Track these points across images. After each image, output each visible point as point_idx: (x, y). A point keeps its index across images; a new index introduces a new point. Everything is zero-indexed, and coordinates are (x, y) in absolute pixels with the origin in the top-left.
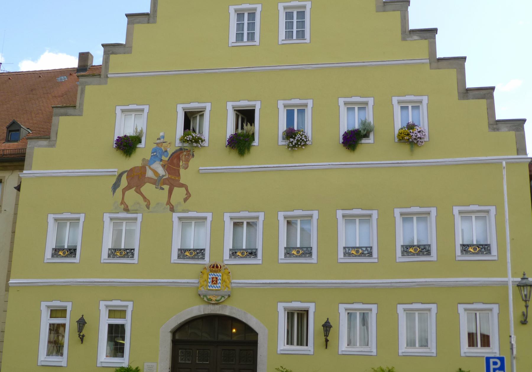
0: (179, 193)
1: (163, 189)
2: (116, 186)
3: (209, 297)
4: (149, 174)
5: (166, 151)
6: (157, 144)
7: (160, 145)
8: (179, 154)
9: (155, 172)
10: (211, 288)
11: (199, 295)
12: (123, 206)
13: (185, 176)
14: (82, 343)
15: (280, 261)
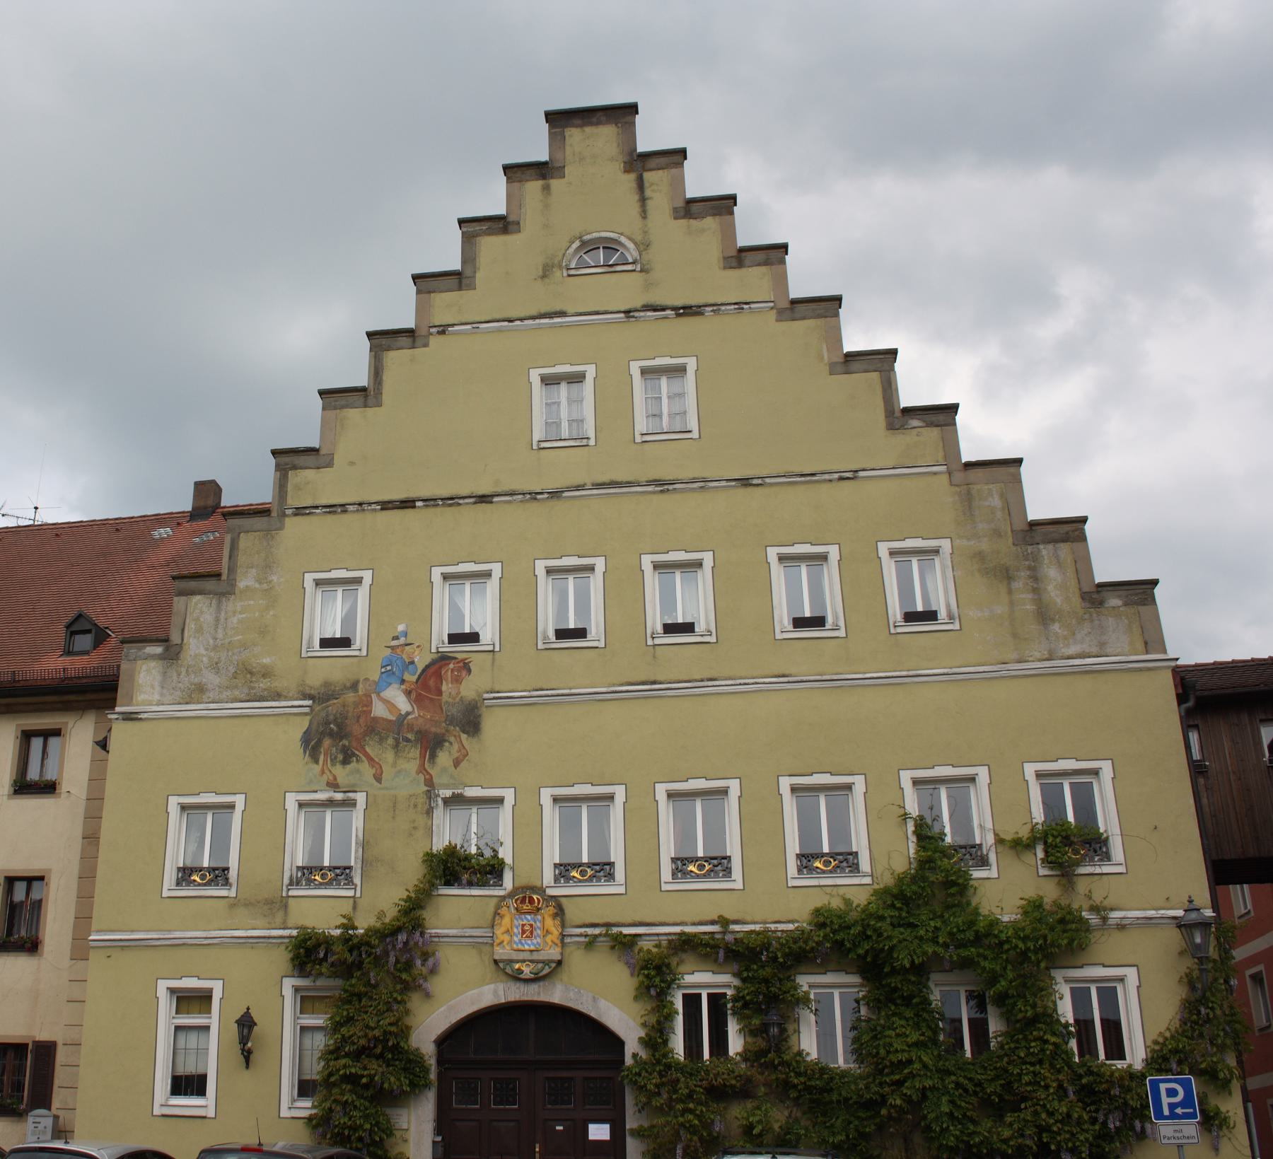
3: (517, 966)
5: (412, 663)
6: (393, 648)
8: (440, 668)
9: (390, 705)
10: (520, 947)
11: (496, 962)
14: (247, 1067)
15: (664, 887)
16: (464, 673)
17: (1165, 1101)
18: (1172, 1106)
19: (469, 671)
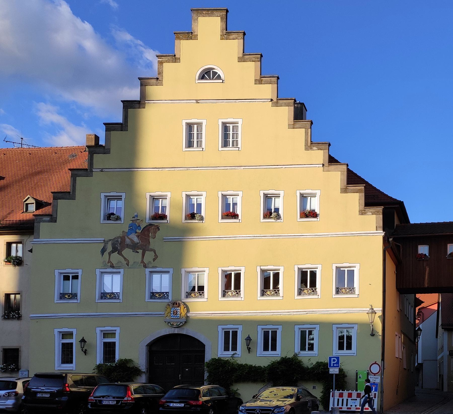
0: (149, 256)
1: (138, 252)
2: (103, 251)
4: (128, 241)
7: (135, 222)
9: (132, 241)
12: (109, 264)
13: (153, 243)
16: (157, 230)
17: (332, 362)
18: (334, 364)
19: (159, 229)
